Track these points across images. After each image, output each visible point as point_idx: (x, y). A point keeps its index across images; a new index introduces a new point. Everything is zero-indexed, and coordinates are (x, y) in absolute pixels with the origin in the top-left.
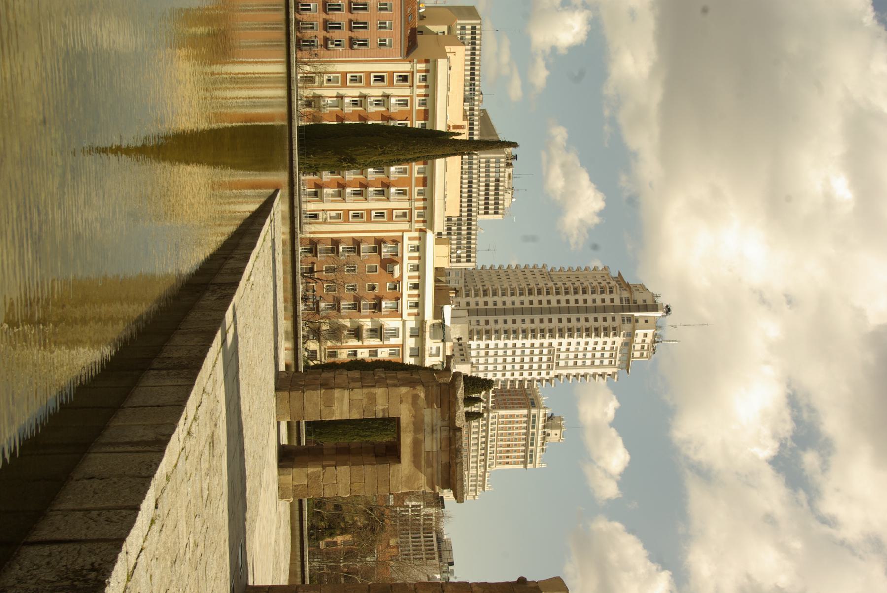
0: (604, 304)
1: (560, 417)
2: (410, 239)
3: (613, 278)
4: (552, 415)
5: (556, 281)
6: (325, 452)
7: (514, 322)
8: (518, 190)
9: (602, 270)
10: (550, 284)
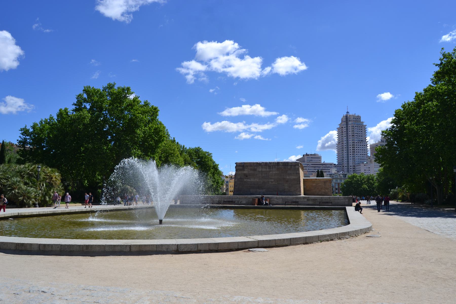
7: (350, 152)
10: (341, 143)
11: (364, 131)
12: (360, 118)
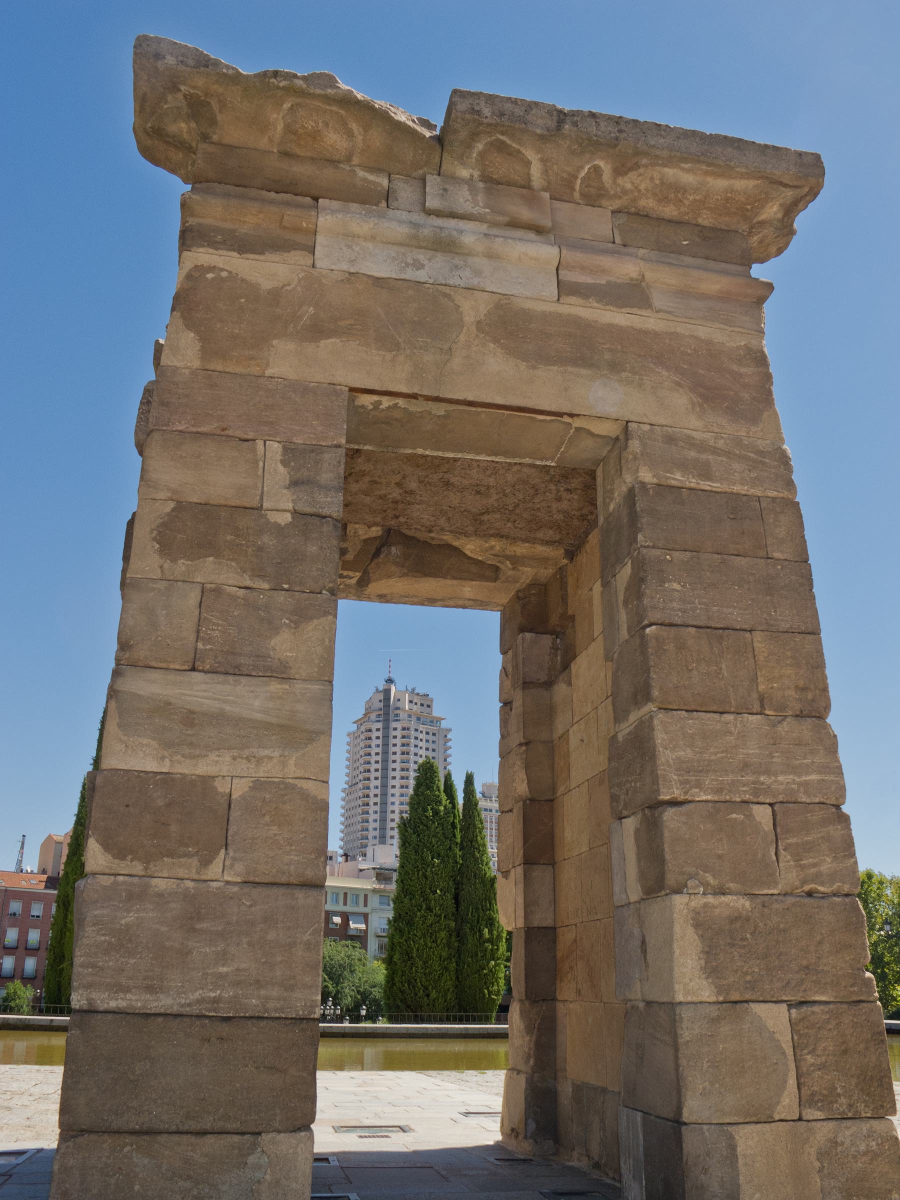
3: (358, 728)
5: (357, 780)
6: (543, 919)
9: (350, 738)
10: (360, 785)
11: (443, 751)
12: (429, 703)
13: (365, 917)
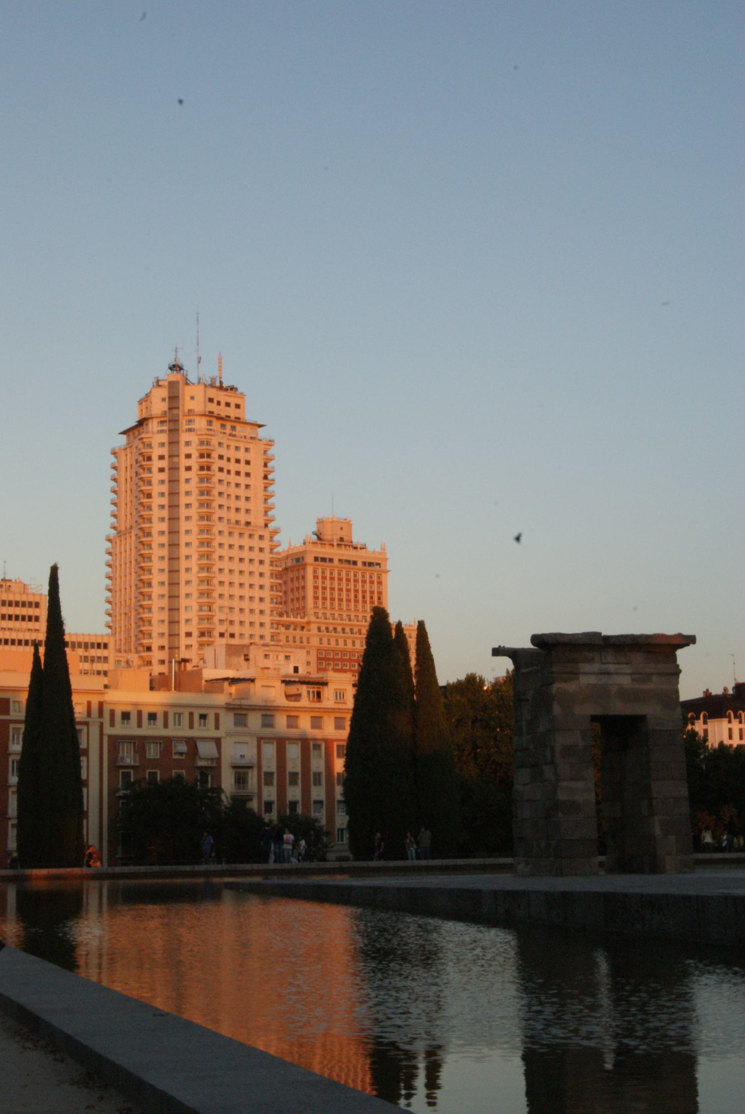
0: (166, 457)
1: (318, 523)
2: (112, 724)
4: (314, 533)
8: (5, 573)
9: (116, 457)
12: (238, 401)
13: (218, 741)
